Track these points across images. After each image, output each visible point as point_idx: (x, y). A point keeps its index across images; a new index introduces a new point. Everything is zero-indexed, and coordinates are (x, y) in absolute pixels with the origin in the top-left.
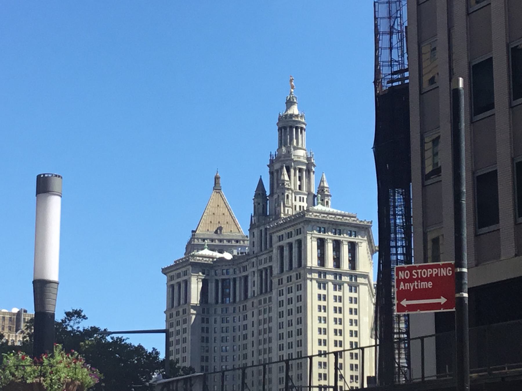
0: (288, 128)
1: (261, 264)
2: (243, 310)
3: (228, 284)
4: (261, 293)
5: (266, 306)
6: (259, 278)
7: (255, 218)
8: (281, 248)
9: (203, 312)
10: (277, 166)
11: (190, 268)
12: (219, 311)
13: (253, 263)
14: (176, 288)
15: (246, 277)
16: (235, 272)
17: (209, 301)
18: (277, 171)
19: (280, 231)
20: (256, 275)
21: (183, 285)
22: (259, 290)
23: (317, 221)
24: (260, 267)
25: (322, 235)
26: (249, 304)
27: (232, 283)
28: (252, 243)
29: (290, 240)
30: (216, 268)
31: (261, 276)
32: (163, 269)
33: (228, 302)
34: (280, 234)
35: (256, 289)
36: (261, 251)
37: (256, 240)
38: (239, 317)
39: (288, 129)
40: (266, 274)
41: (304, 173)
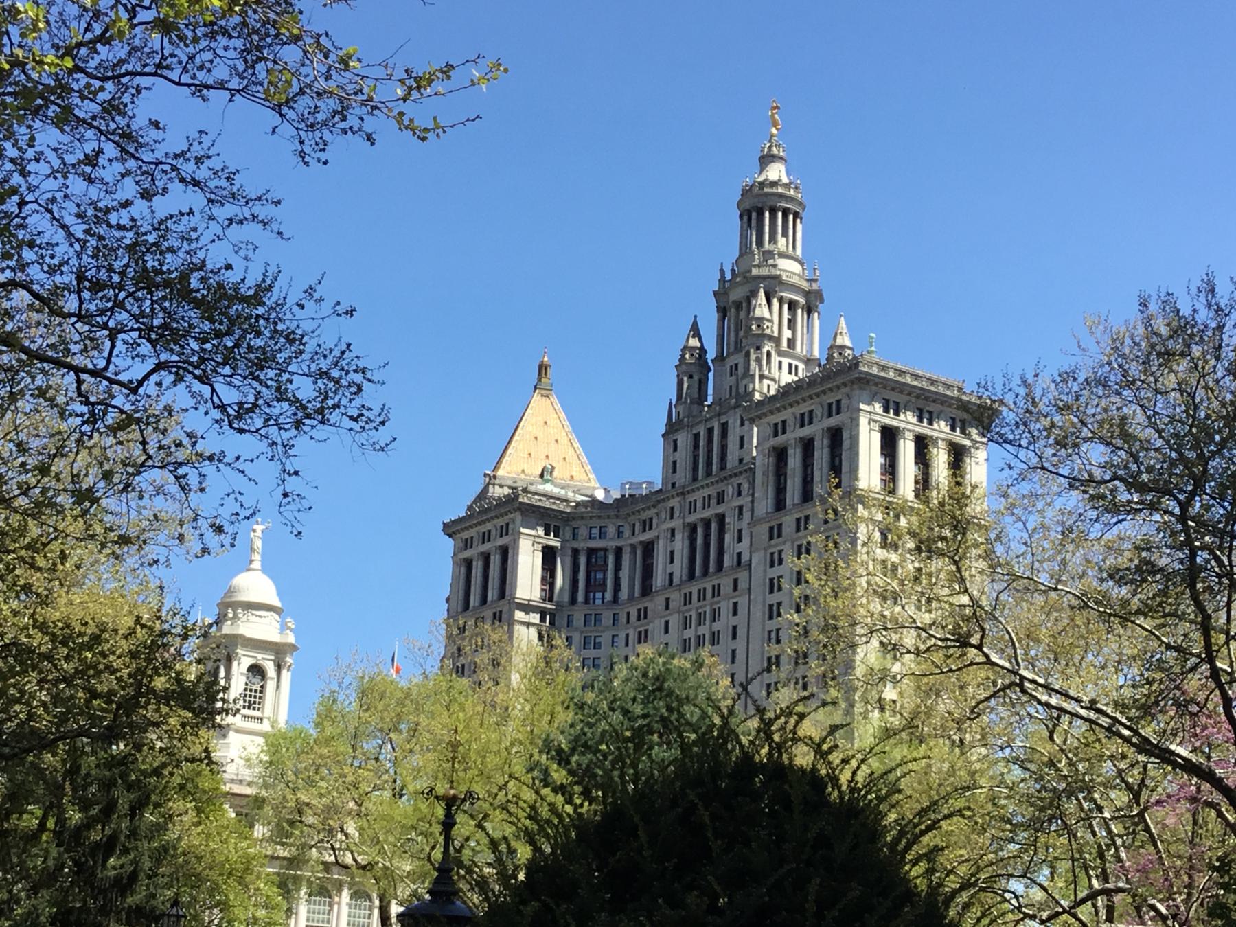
0: (760, 209)
1: (692, 508)
2: (639, 619)
3: (601, 562)
4: (691, 576)
5: (690, 610)
6: (687, 543)
7: (680, 408)
10: (736, 294)
11: (518, 517)
13: (672, 509)
14: (478, 566)
15: (648, 549)
16: (620, 534)
18: (738, 305)
19: (779, 410)
20: (678, 536)
21: (495, 560)
22: (685, 571)
23: (885, 383)
24: (692, 519)
25: (890, 420)
26: (655, 604)
27: (611, 559)
28: (671, 464)
29: (806, 431)
30: (574, 524)
32: (445, 525)
33: (598, 602)
34: (777, 418)
35: (679, 568)
36: (695, 479)
37: (683, 456)
38: (627, 635)
40: (707, 536)
41: (799, 311)
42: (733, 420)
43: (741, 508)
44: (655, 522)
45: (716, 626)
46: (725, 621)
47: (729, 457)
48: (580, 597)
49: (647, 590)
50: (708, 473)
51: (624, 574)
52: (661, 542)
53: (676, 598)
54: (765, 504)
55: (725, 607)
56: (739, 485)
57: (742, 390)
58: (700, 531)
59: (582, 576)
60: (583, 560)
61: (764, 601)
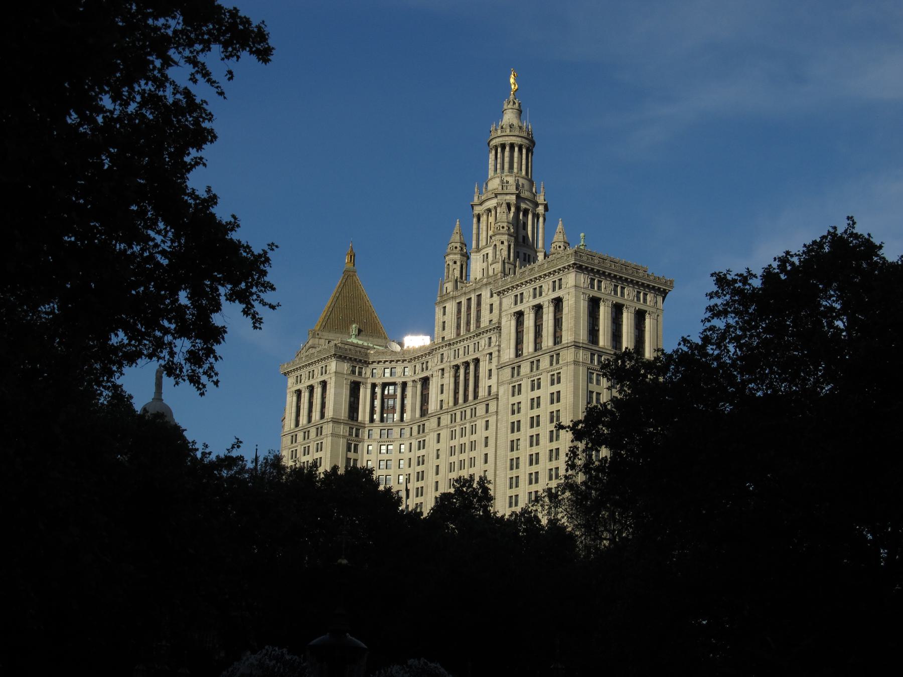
2: (419, 433)
4: (456, 402)
6: (452, 380)
8: (520, 315)
9: (351, 434)
12: (376, 433)
14: (305, 396)
15: (425, 381)
17: (360, 418)
18: (489, 210)
20: (446, 375)
21: (318, 391)
30: (375, 365)
31: (456, 377)
39: (507, 149)
40: (467, 374)
42: (485, 294)
43: (491, 354)
44: (429, 364)
45: (473, 438)
46: (481, 433)
47: (482, 320)
48: (376, 417)
49: (424, 412)
50: (468, 330)
51: (408, 402)
52: (434, 379)
53: (446, 419)
54: (509, 353)
55: (480, 424)
56: (490, 338)
57: (491, 273)
58: (462, 371)
59: (377, 403)
60: (378, 390)
61: (507, 421)
